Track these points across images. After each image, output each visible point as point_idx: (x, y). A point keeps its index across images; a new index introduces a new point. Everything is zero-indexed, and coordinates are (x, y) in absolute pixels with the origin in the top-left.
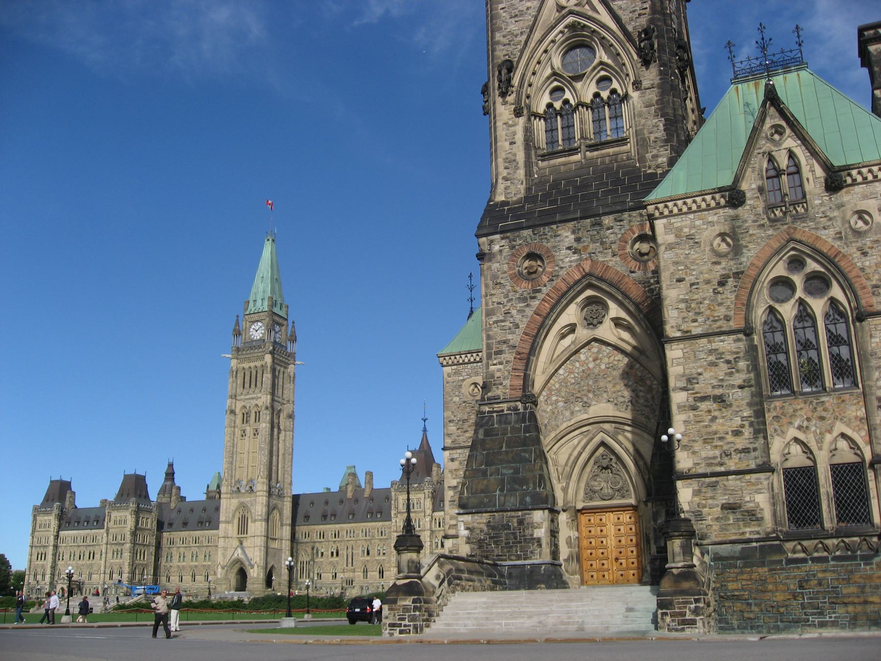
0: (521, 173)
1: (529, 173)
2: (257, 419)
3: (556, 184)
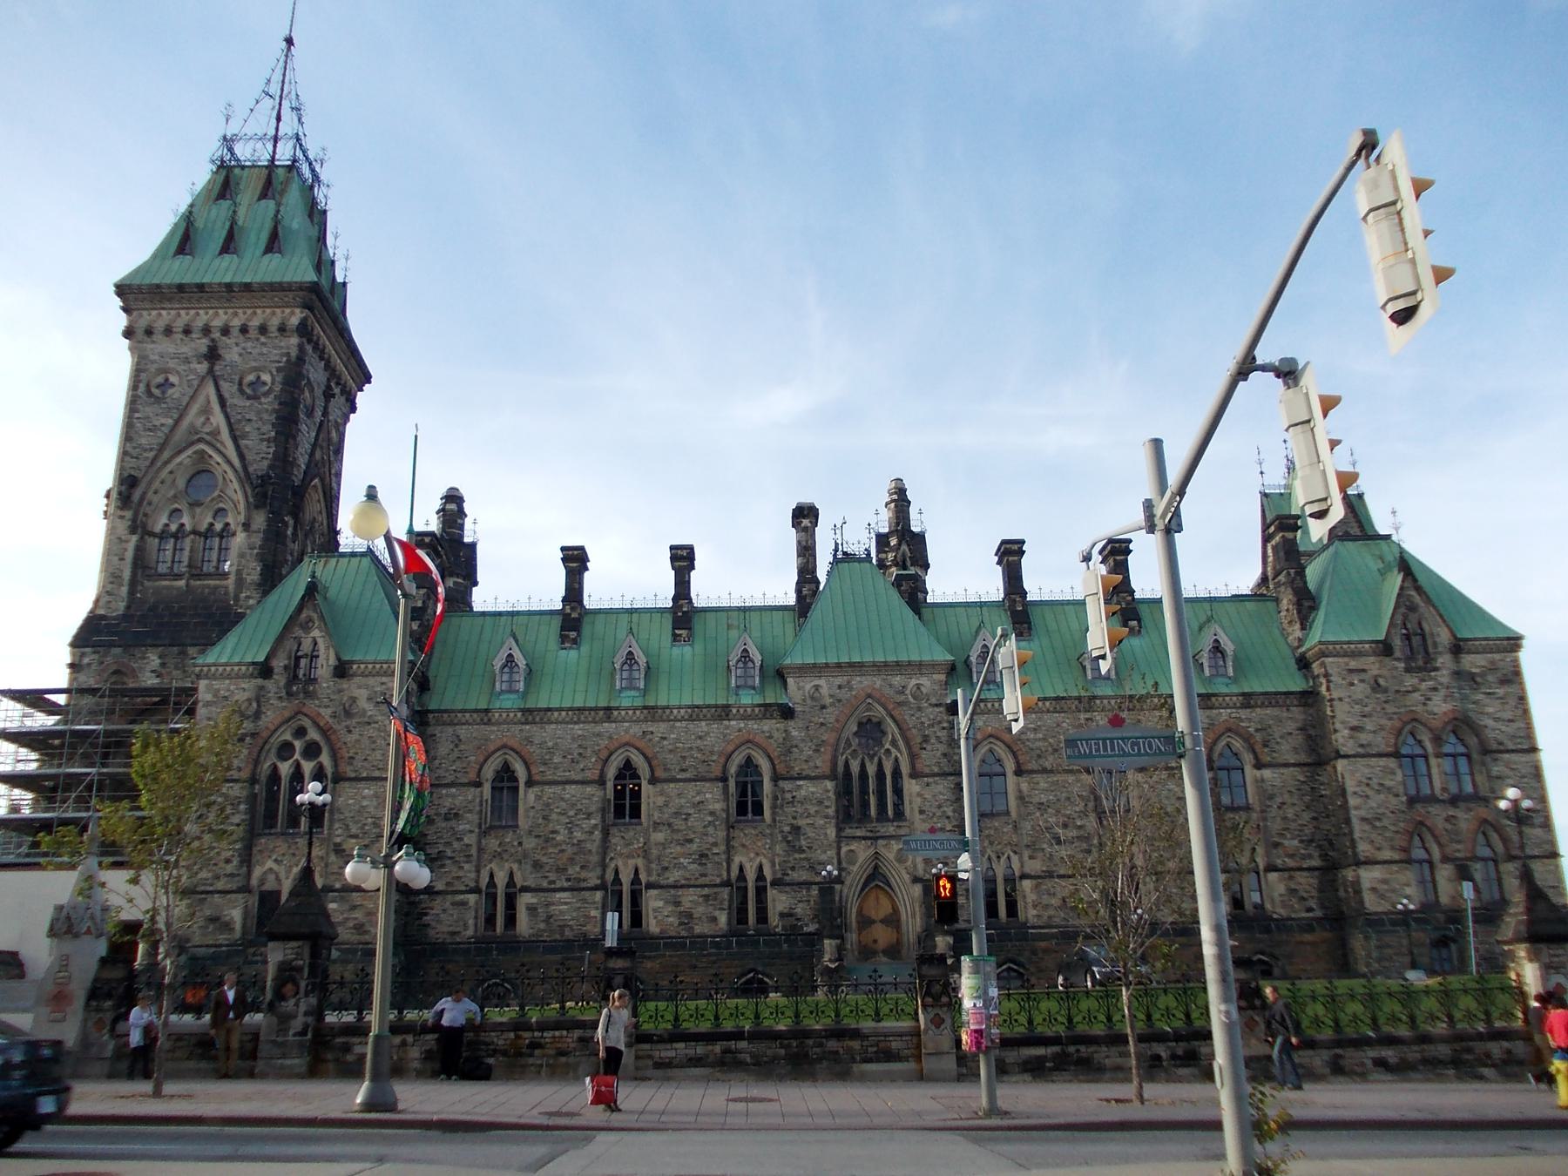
0: (124, 590)
1: (132, 592)
3: (153, 608)
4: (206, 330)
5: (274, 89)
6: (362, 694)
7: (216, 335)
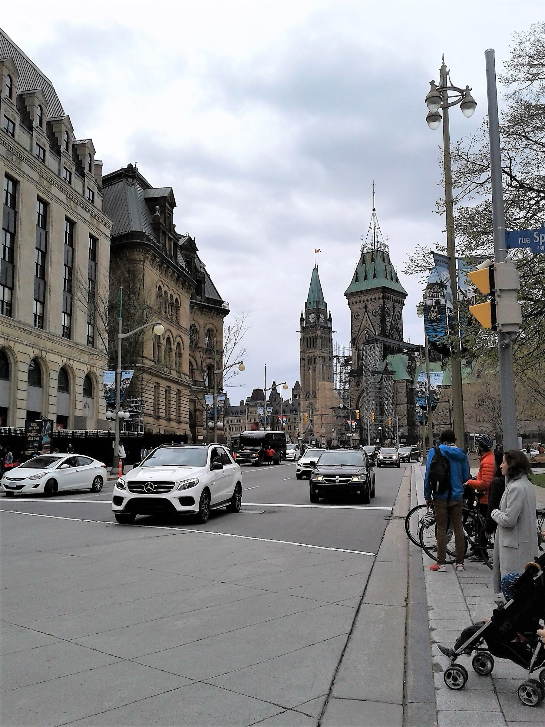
2: (315, 362)
4: (364, 301)
5: (372, 226)
6: (398, 387)
7: (366, 302)
